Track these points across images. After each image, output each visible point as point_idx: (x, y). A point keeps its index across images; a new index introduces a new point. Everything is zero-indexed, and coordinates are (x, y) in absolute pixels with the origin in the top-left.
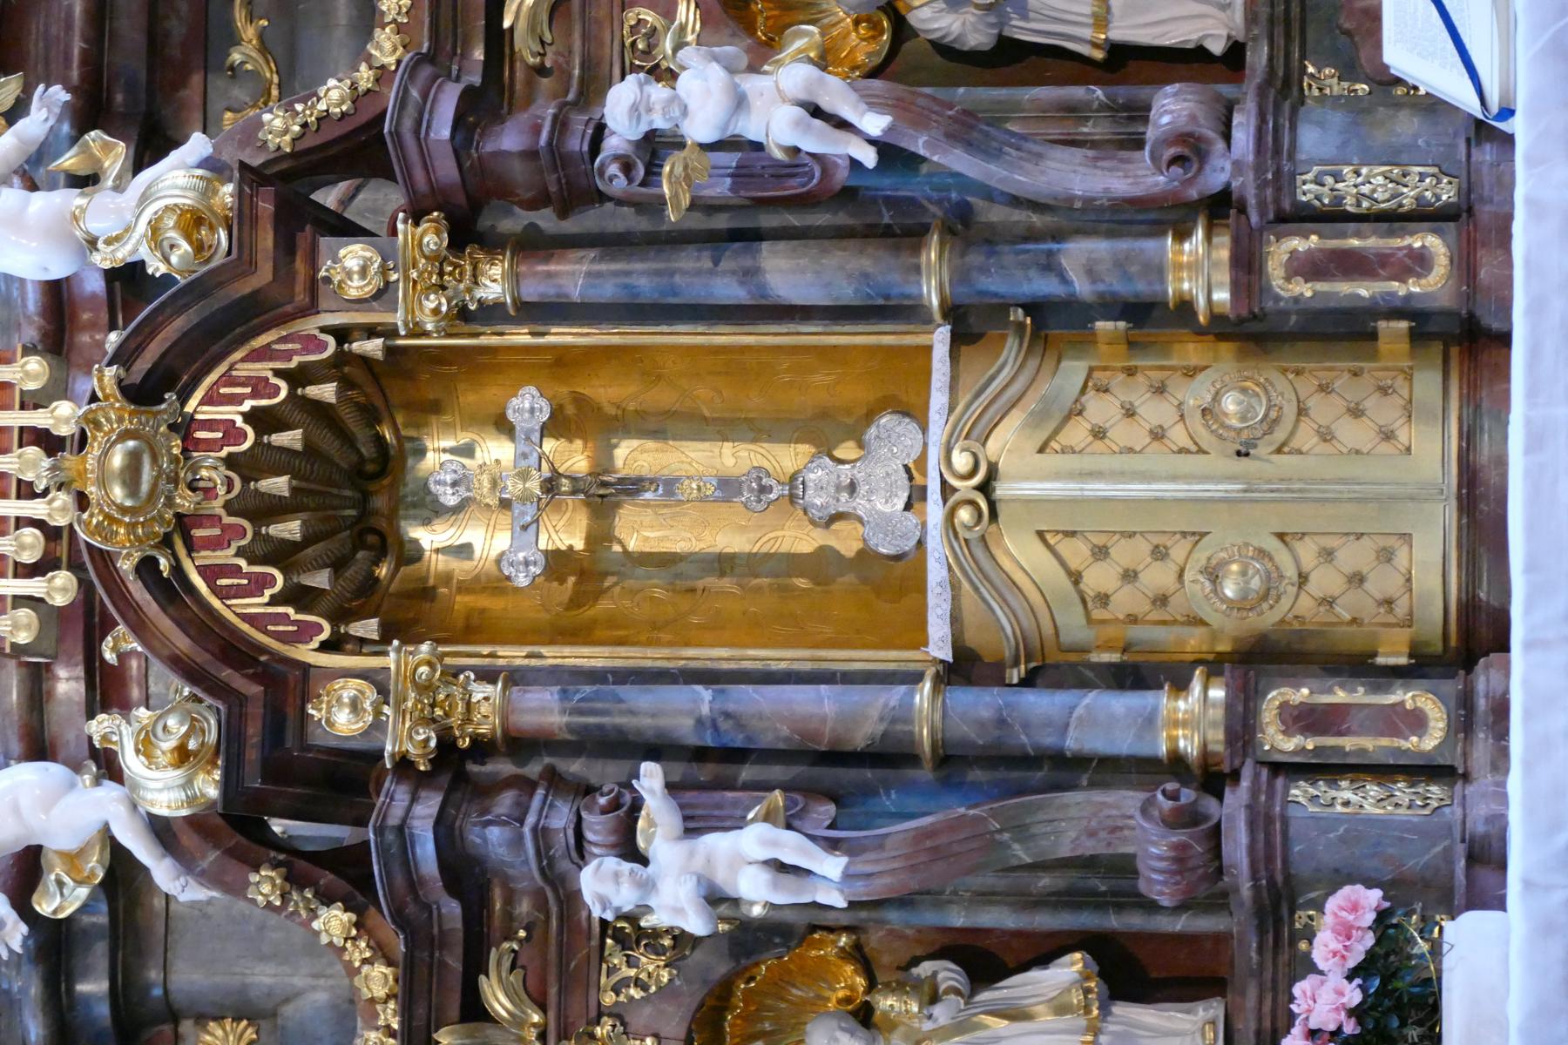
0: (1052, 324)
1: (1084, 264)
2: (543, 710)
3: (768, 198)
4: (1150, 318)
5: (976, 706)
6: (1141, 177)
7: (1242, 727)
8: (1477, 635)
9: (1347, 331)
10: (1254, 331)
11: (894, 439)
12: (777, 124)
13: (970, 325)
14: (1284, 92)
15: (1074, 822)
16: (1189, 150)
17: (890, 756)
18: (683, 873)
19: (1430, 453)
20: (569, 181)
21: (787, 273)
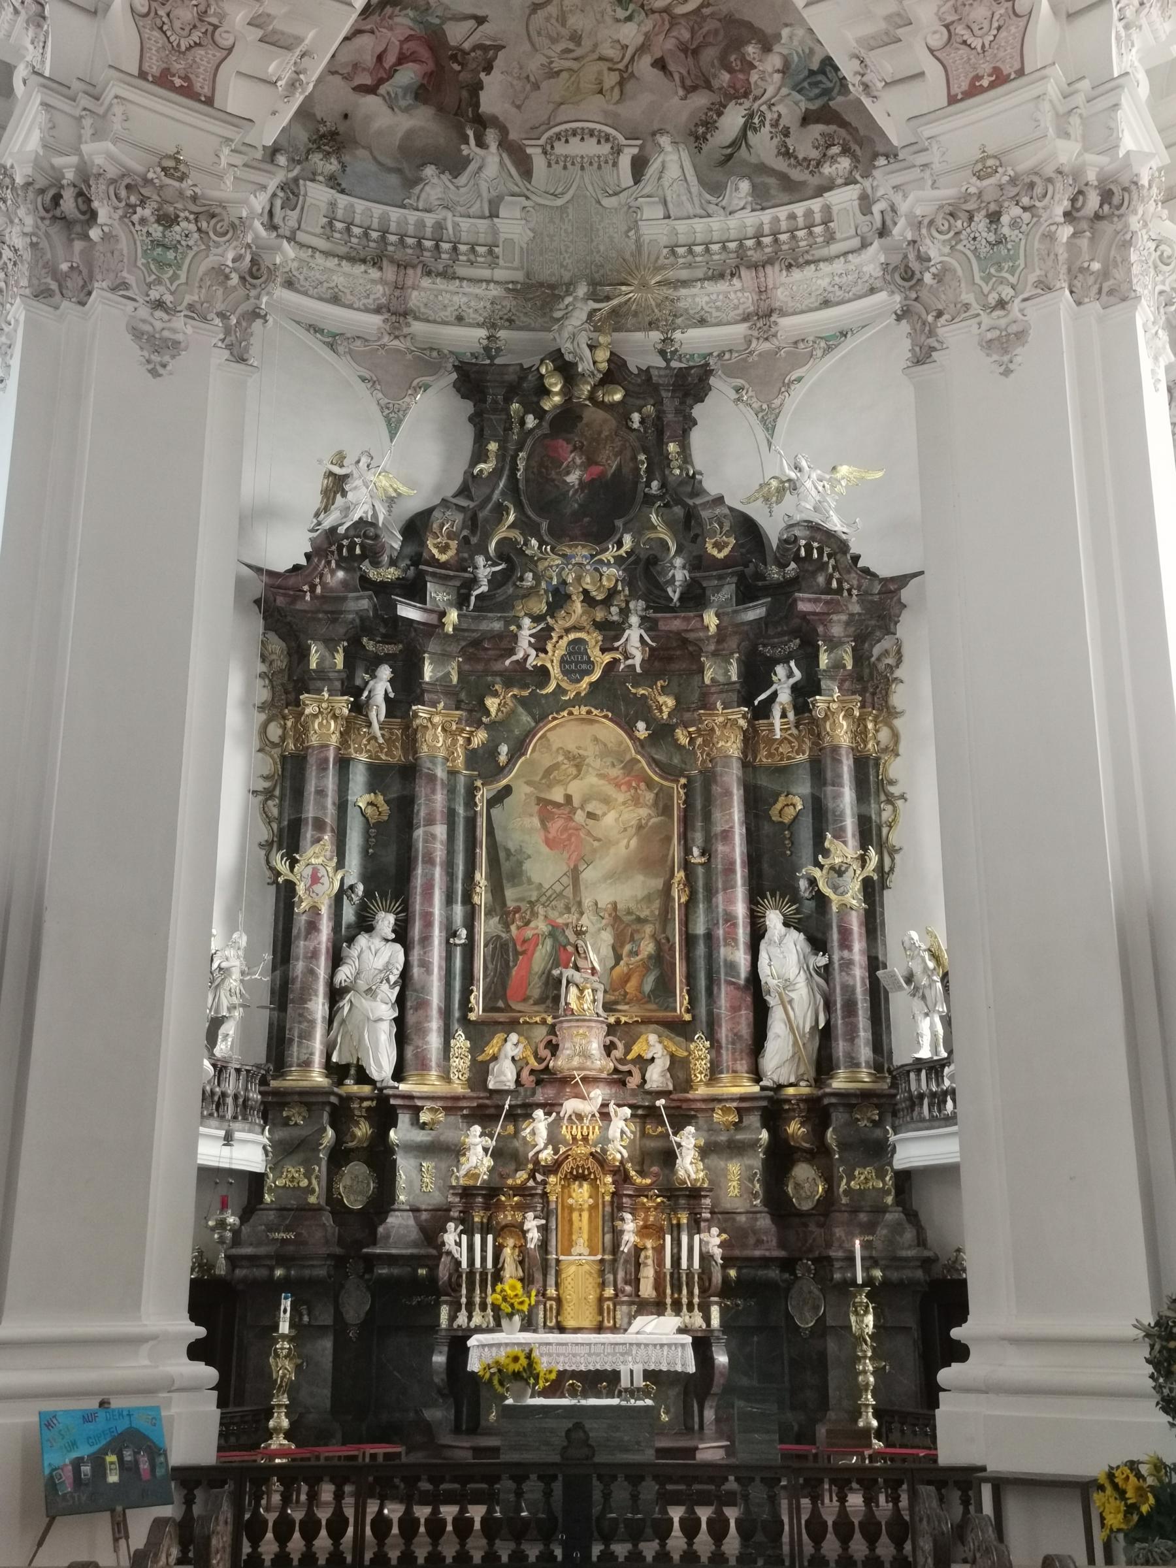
0: (602, 1273)
1: (610, 1277)
2: (553, 1206)
3: (617, 1234)
4: (603, 1285)
5: (553, 1263)
6: (620, 1284)
7: (550, 1299)
8: (561, 1329)
9: (600, 1312)
10: (601, 1300)
11: (586, 1251)
12: (626, 1237)
13: (602, 1261)
14: (631, 1303)
15: (538, 1276)
16: (623, 1291)
17: (547, 1252)
18: (532, 1224)
19: (586, 1324)
20: (621, 1208)
21: (608, 1237)
